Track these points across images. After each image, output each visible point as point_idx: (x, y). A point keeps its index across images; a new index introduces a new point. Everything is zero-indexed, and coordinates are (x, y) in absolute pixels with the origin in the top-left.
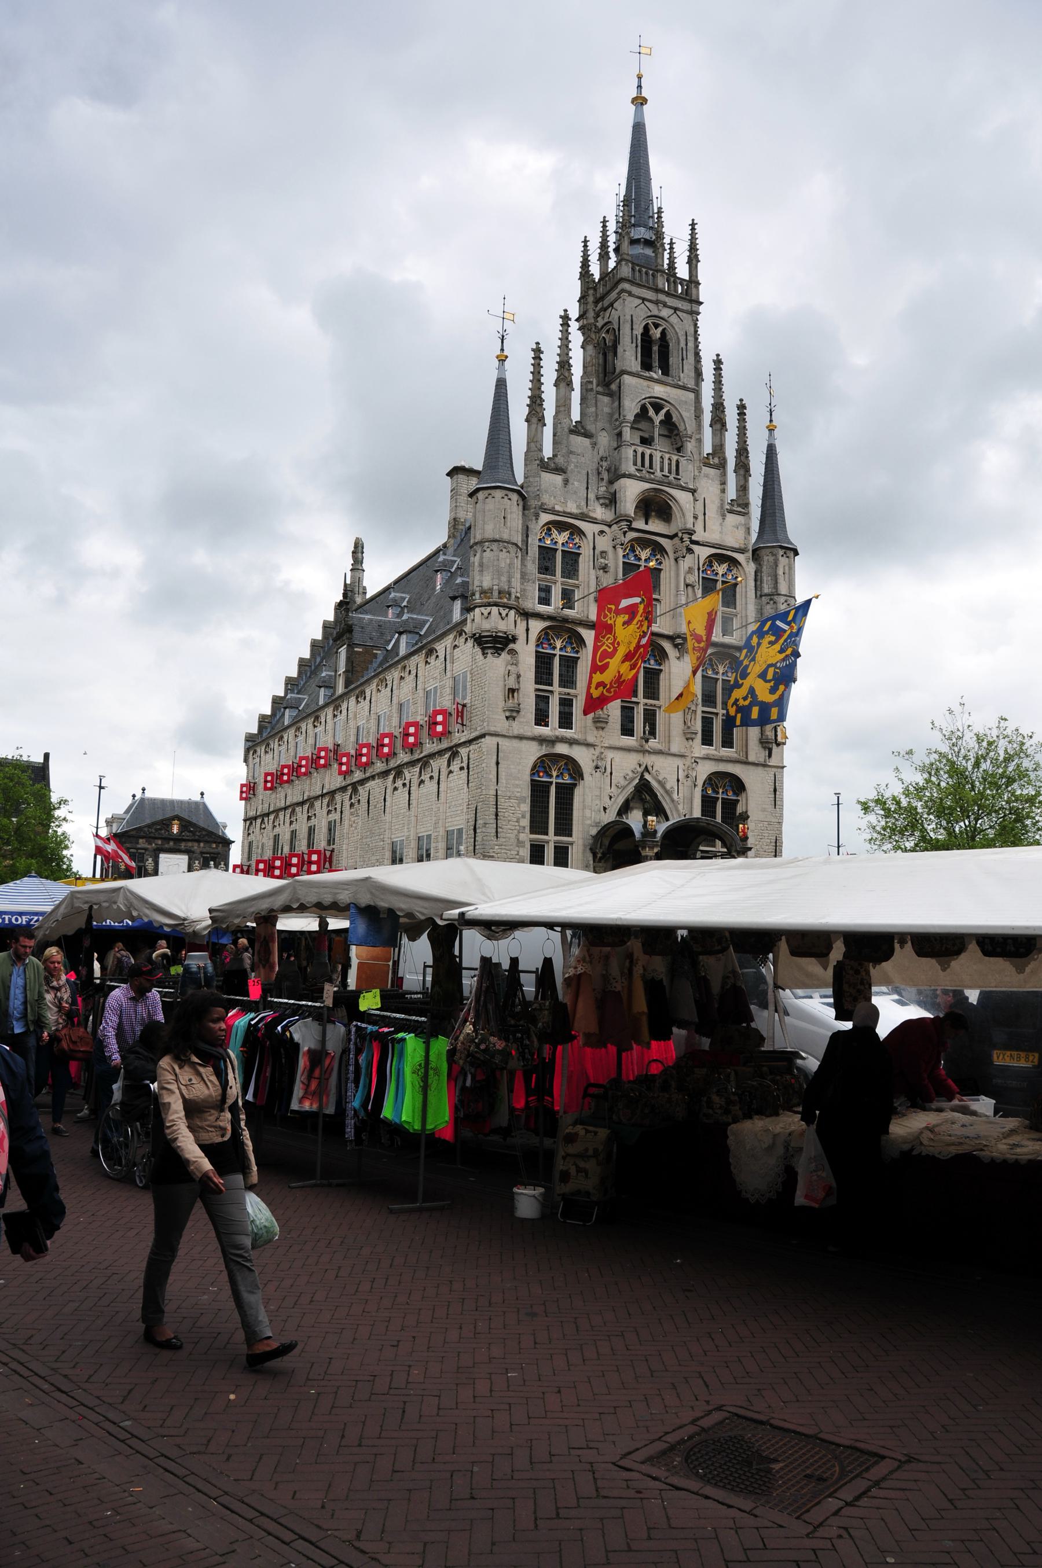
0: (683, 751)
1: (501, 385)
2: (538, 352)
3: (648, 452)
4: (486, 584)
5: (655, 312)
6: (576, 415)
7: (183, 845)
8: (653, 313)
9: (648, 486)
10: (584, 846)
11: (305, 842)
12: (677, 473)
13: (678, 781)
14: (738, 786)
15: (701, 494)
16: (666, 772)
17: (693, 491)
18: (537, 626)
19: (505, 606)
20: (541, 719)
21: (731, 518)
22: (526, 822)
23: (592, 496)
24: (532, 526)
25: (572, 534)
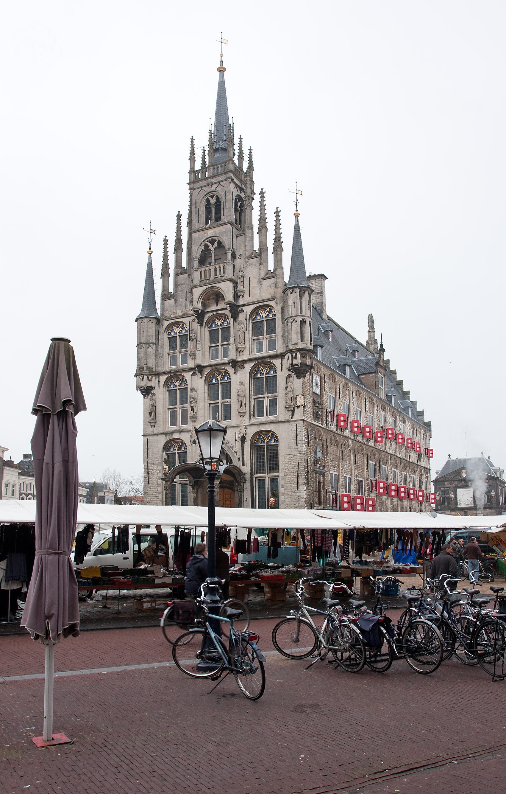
0: (239, 423)
1: (150, 266)
2: (166, 240)
3: (207, 269)
5: (209, 190)
8: (207, 192)
9: (205, 287)
12: (224, 273)
13: (236, 440)
18: (163, 378)
25: (183, 326)
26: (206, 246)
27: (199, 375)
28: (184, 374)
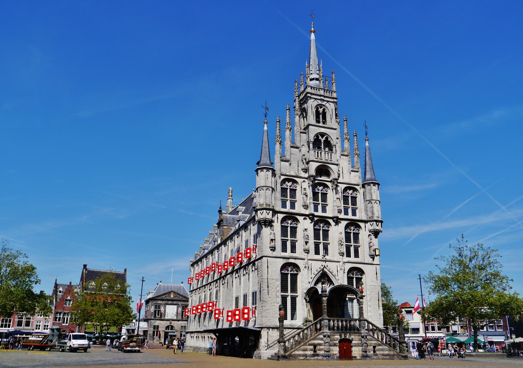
4: (261, 202)
7: (175, 302)
10: (302, 297)
11: (208, 299)
14: (361, 272)
15: (341, 165)
16: (332, 267)
17: (337, 165)
18: (281, 216)
20: (284, 250)
22: (279, 288)
23: (300, 169)
26: (318, 137)
27: (308, 220)
28: (298, 217)
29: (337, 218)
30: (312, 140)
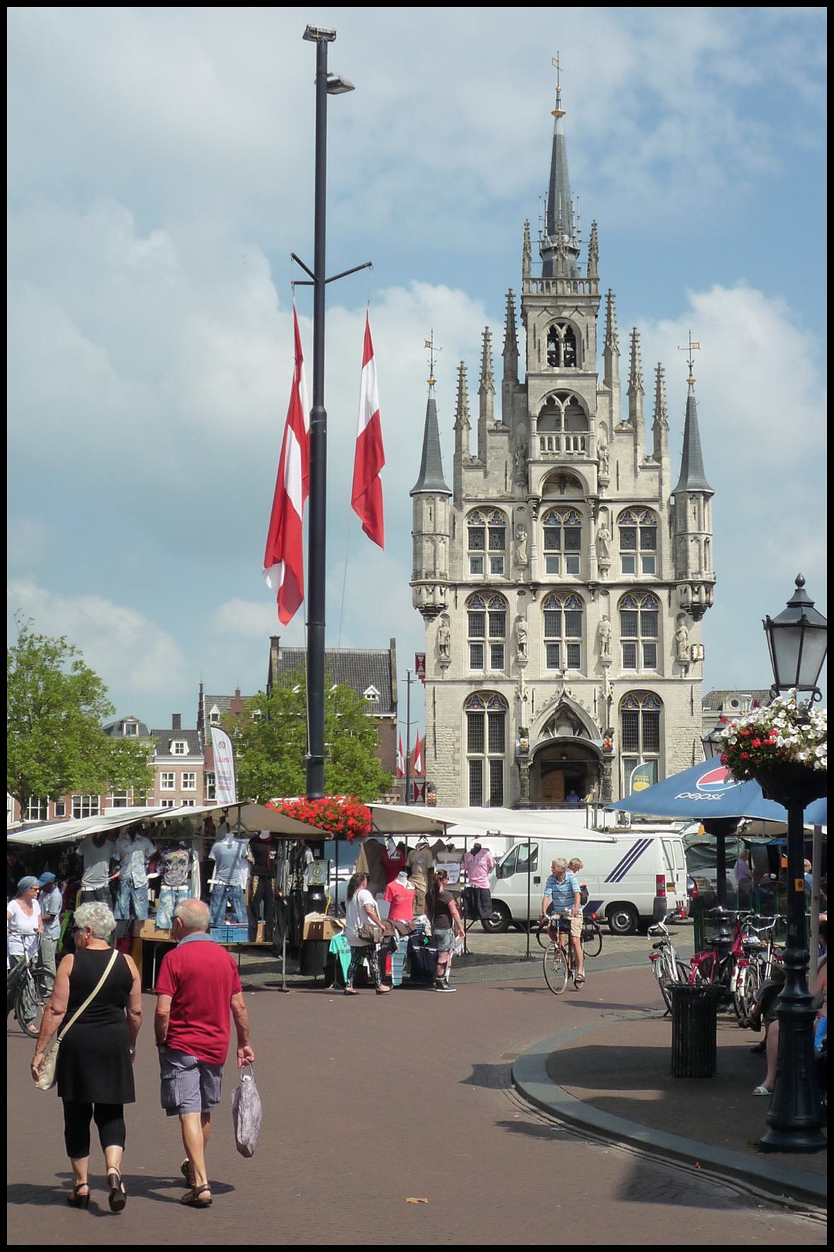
0: (599, 677)
1: (431, 405)
6: (498, 416)
14: (658, 701)
18: (464, 594)
19: (430, 584)
20: (477, 662)
21: (643, 475)
24: (458, 514)
29: (597, 584)
30: (536, 409)
